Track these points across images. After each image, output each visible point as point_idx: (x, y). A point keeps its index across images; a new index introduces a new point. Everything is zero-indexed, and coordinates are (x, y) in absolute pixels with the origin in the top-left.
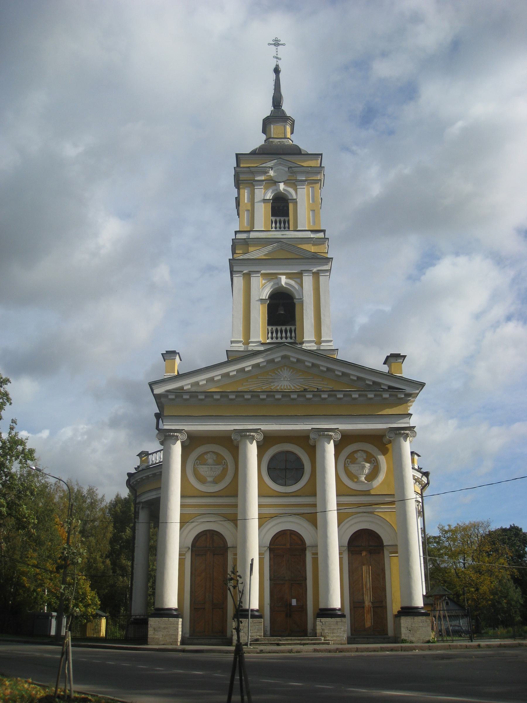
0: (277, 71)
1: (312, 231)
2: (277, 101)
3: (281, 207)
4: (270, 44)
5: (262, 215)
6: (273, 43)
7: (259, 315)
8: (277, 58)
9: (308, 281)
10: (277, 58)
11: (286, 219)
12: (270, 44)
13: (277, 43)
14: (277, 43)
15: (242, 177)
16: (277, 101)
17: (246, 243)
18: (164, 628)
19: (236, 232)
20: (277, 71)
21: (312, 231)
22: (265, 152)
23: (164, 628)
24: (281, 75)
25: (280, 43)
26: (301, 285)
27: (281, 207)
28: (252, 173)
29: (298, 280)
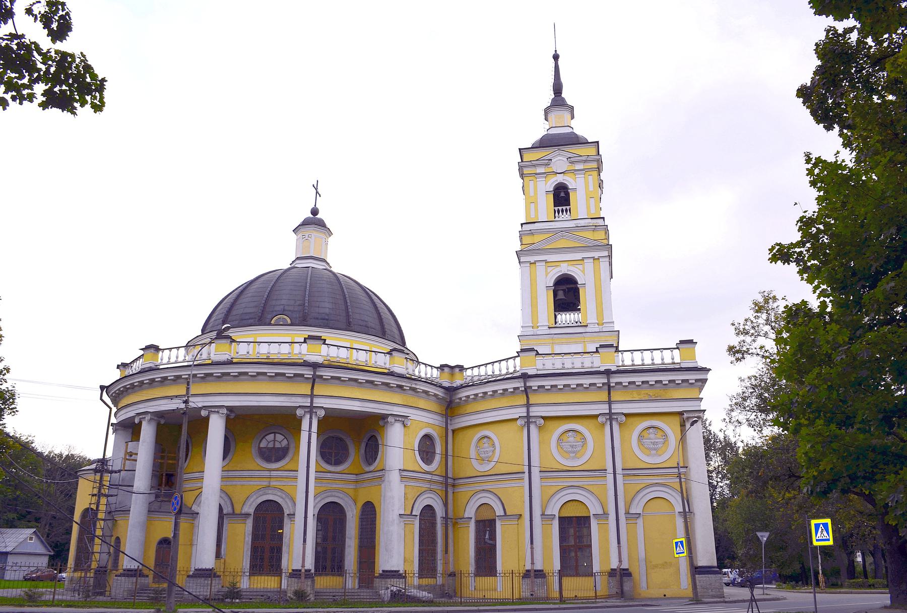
0: (556, 57)
2: (558, 89)
3: (561, 197)
5: (546, 203)
7: (546, 300)
9: (589, 265)
15: (526, 171)
16: (558, 89)
17: (531, 233)
19: (522, 224)
20: (556, 57)
22: (546, 143)
24: (561, 62)
26: (583, 271)
27: (561, 197)
29: (580, 267)
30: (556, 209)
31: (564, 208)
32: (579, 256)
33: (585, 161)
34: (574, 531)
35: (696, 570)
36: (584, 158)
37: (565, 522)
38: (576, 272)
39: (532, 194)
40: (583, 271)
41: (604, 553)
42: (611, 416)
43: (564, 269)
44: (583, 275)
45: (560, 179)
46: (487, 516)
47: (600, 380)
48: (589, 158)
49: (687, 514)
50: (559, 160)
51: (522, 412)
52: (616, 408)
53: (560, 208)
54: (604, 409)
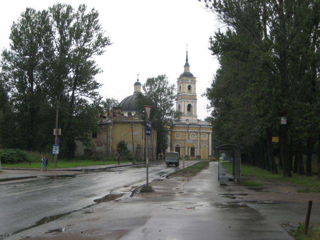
0: (187, 52)
9: (194, 103)
16: (187, 60)
20: (187, 52)
26: (193, 104)
27: (189, 88)
32: (192, 101)
34: (193, 150)
35: (209, 156)
37: (191, 148)
38: (191, 104)
39: (184, 86)
40: (193, 104)
41: (197, 153)
42: (200, 132)
43: (190, 103)
44: (193, 105)
45: (190, 84)
46: (179, 147)
47: (199, 126)
49: (208, 148)
51: (187, 130)
52: (201, 131)
54: (199, 131)
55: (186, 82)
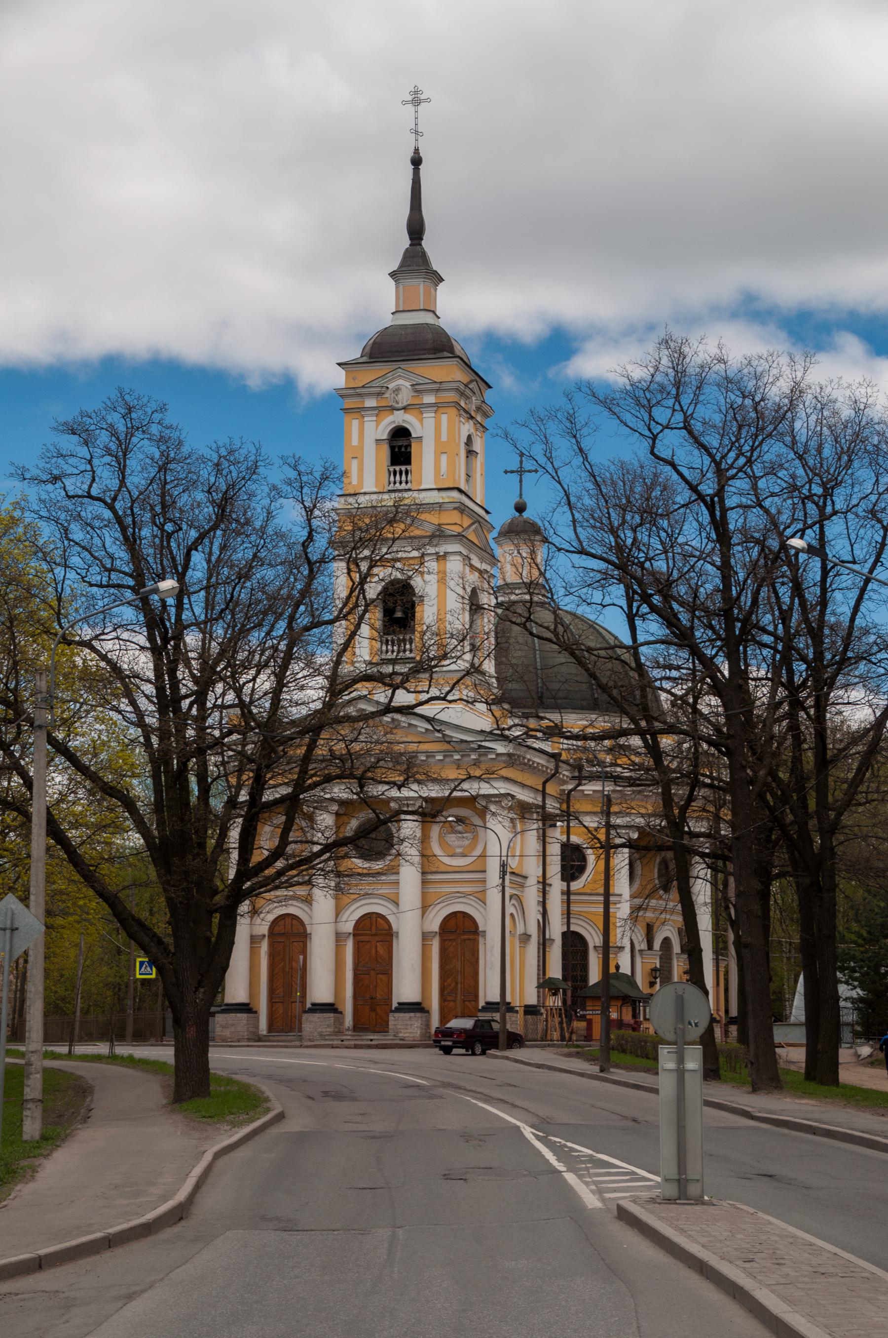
0: (416, 162)
1: (439, 490)
4: (404, 103)
6: (410, 98)
8: (416, 132)
10: (416, 132)
11: (409, 468)
12: (404, 103)
13: (416, 100)
14: (416, 100)
18: (232, 1025)
20: (416, 162)
21: (439, 490)
23: (232, 1025)
25: (422, 97)
28: (360, 395)
30: (392, 469)
31: (403, 468)
33: (438, 390)
36: (436, 386)
48: (444, 386)
50: (401, 383)
53: (397, 468)
55: (371, 403)
